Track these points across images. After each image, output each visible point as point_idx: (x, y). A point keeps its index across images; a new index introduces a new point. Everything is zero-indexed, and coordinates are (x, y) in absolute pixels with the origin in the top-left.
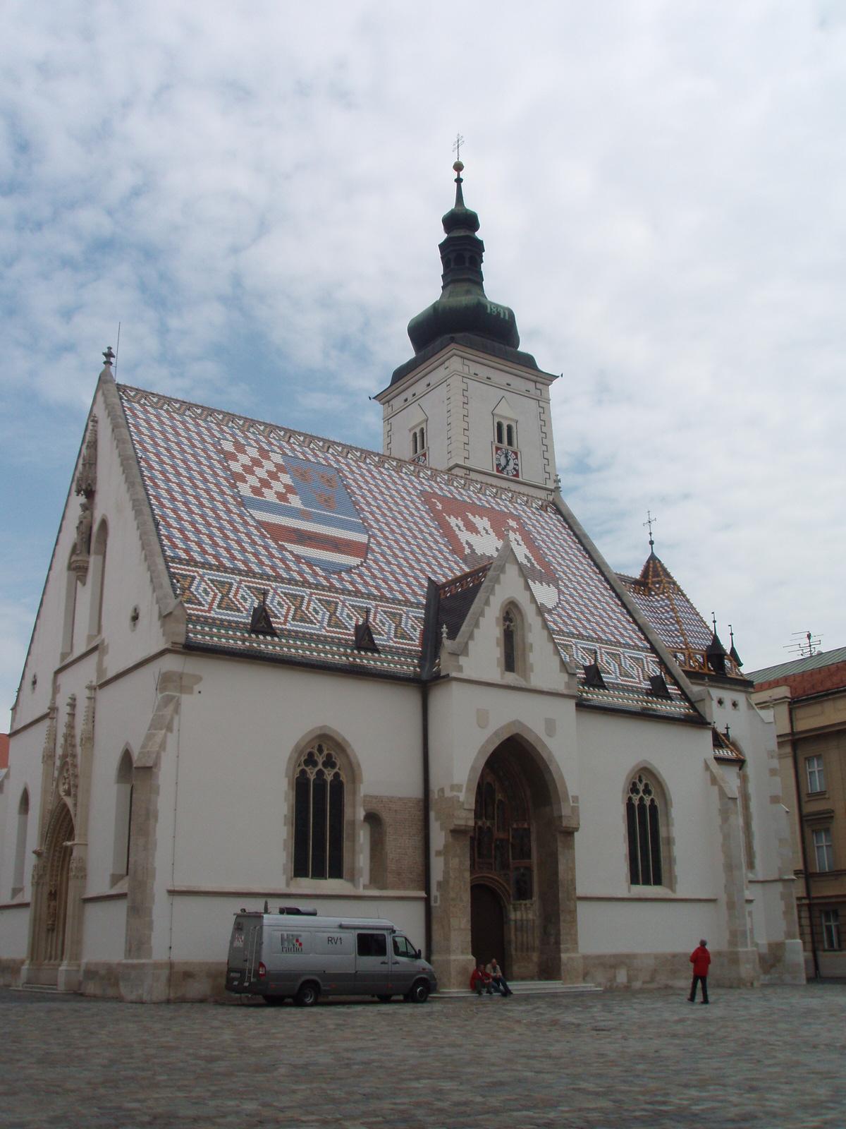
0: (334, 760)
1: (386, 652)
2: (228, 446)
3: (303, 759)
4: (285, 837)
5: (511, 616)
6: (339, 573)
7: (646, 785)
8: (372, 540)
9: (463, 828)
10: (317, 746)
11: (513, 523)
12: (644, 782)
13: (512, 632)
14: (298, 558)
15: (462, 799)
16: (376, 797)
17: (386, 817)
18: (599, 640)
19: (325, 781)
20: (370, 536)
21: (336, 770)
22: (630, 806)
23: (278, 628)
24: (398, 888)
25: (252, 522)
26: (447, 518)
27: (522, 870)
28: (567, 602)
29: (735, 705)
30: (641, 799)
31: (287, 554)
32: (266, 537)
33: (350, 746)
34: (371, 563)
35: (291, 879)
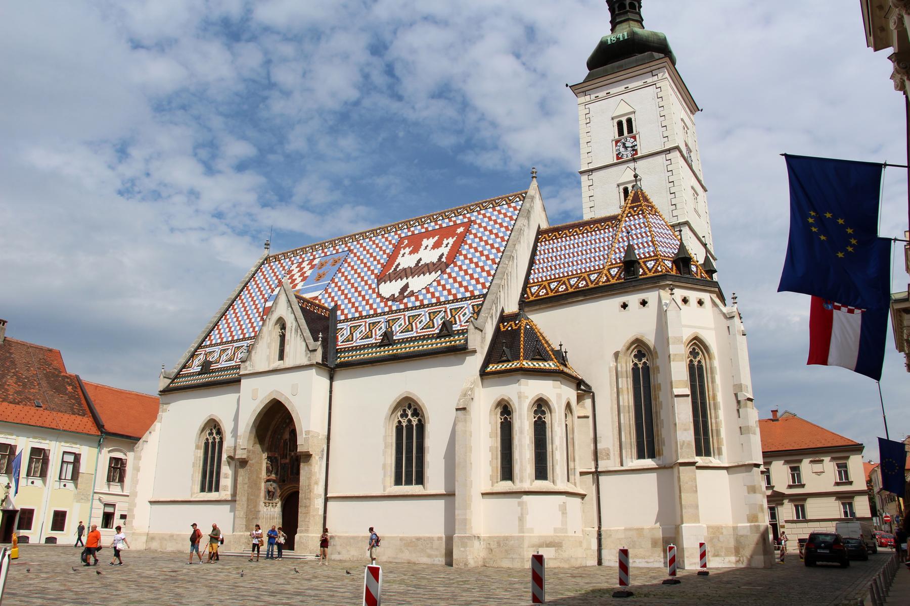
7: (415, 410)
12: (413, 407)
18: (439, 303)
22: (399, 429)
25: (261, 310)
29: (644, 303)
30: (409, 421)
35: (197, 493)
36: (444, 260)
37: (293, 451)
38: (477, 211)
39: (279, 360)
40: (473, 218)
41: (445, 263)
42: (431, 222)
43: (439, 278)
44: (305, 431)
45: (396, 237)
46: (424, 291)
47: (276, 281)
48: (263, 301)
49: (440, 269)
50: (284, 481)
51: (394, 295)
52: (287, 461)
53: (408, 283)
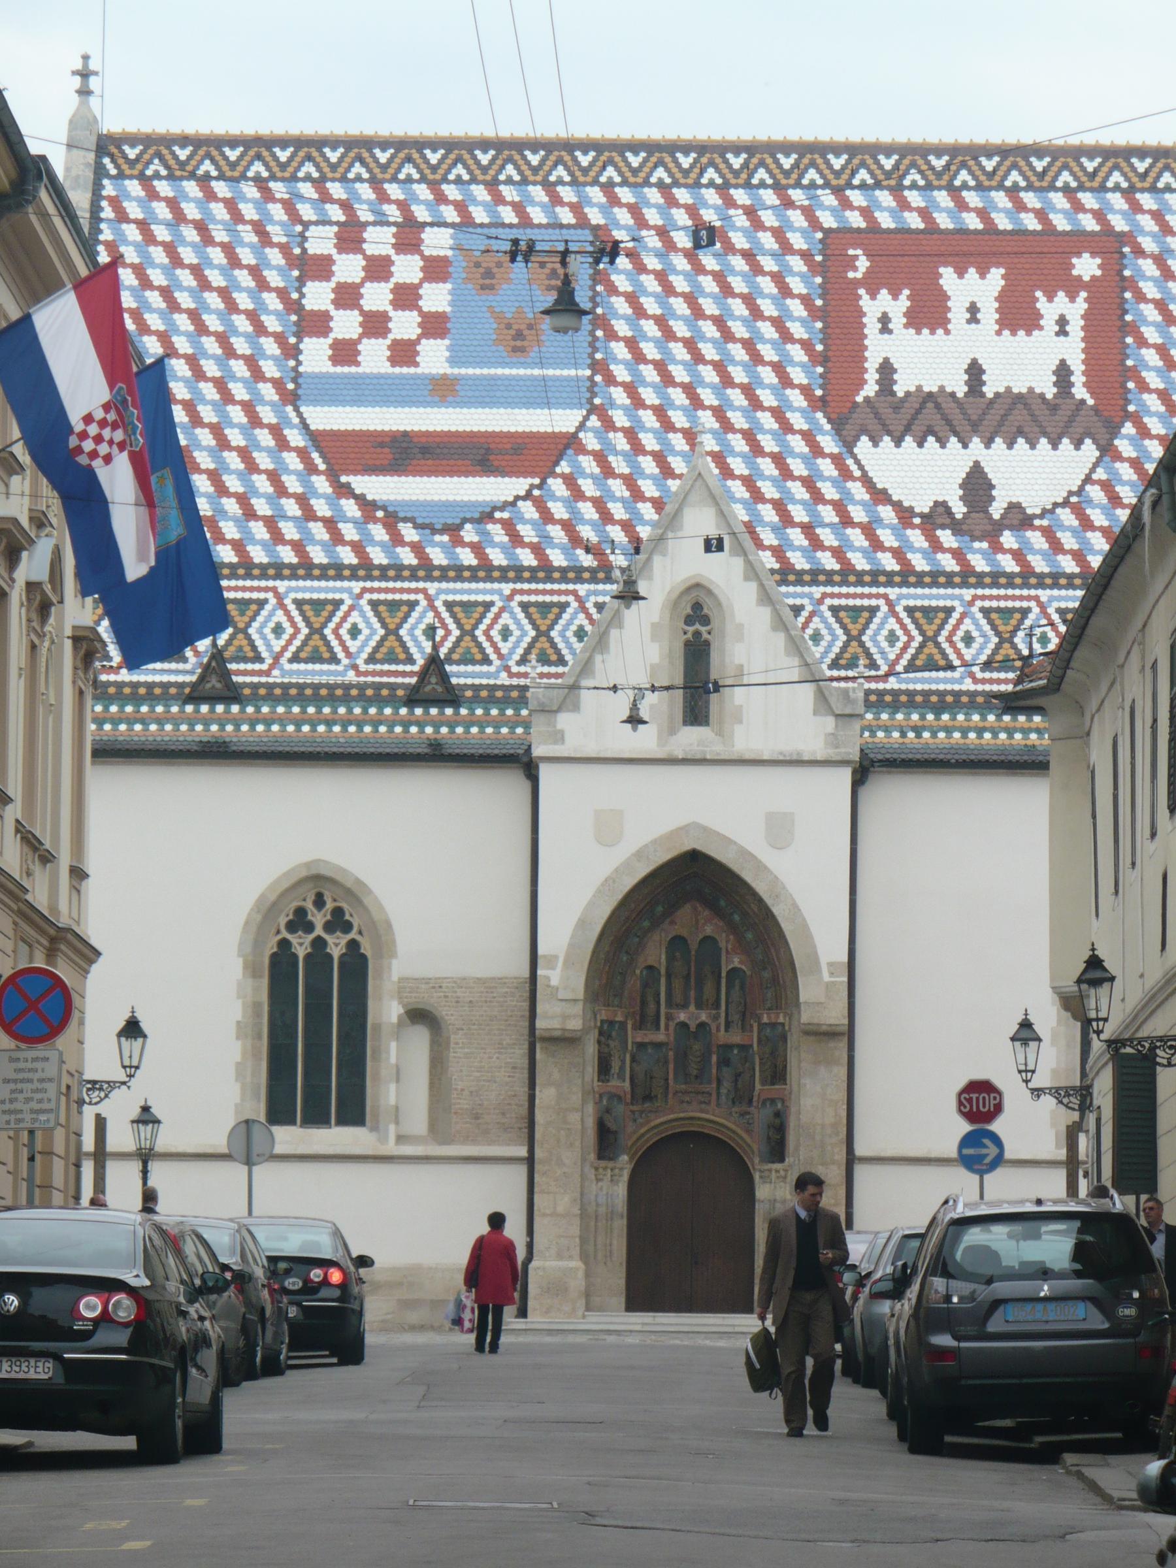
0: (347, 917)
1: (476, 700)
2: (321, 242)
3: (283, 921)
4: (239, 1059)
5: (705, 611)
6: (453, 530)
8: (594, 421)
9: (557, 1034)
10: (311, 897)
11: (1086, 266)
13: (707, 644)
14: (368, 507)
15: (555, 981)
16: (427, 981)
17: (449, 1015)
19: (330, 957)
20: (593, 410)
21: (353, 935)
23: (245, 685)
24: (474, 1142)
25: (296, 438)
26: (865, 302)
27: (779, 1105)
28: (1107, 487)
31: (350, 507)
32: (312, 469)
33: (369, 892)
34: (557, 486)
36: (1080, 392)
37: (684, 1006)
38: (1117, 188)
39: (685, 723)
40: (1119, 224)
41: (1095, 409)
42: (929, 187)
43: (1100, 474)
44: (830, 965)
45: (797, 218)
46: (1066, 516)
47: (272, 301)
48: (267, 391)
49: (1089, 434)
50: (648, 1098)
51: (942, 508)
52: (661, 1037)
53: (977, 464)
